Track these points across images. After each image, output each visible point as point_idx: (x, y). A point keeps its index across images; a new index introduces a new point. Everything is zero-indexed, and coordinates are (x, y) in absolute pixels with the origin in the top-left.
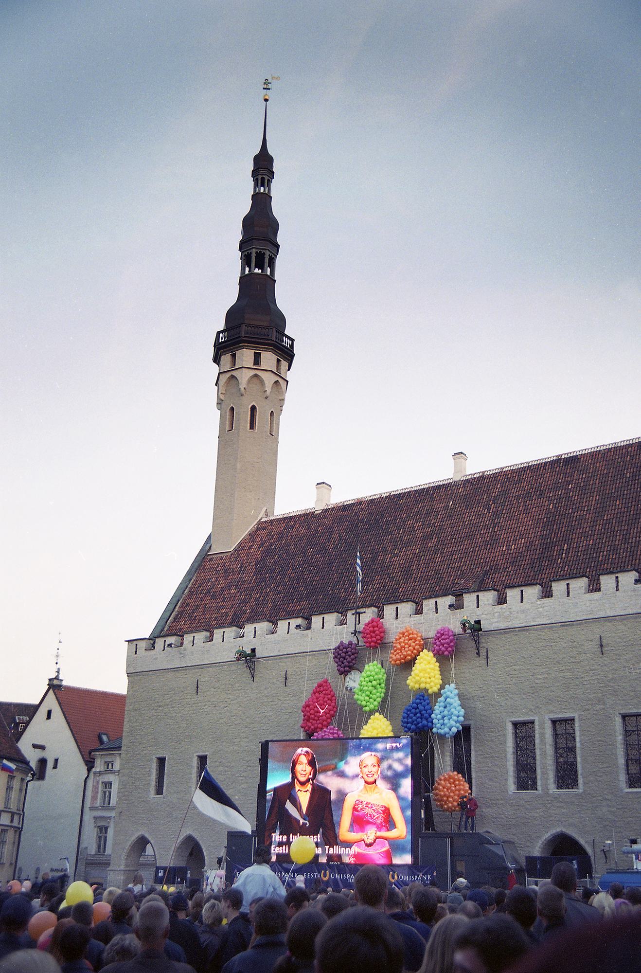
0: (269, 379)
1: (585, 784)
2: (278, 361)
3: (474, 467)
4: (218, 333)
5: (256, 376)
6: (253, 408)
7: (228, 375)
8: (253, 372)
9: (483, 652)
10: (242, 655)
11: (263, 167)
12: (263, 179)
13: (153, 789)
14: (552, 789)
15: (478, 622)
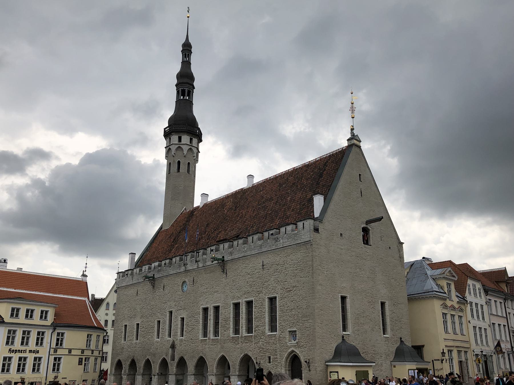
0: (185, 148)
1: (255, 331)
2: (191, 140)
3: (257, 180)
4: (165, 129)
5: (179, 147)
6: (179, 162)
7: (168, 148)
8: (178, 146)
9: (225, 270)
10: (146, 277)
11: (187, 49)
12: (188, 55)
13: (123, 339)
14: (245, 334)
15: (223, 257)
